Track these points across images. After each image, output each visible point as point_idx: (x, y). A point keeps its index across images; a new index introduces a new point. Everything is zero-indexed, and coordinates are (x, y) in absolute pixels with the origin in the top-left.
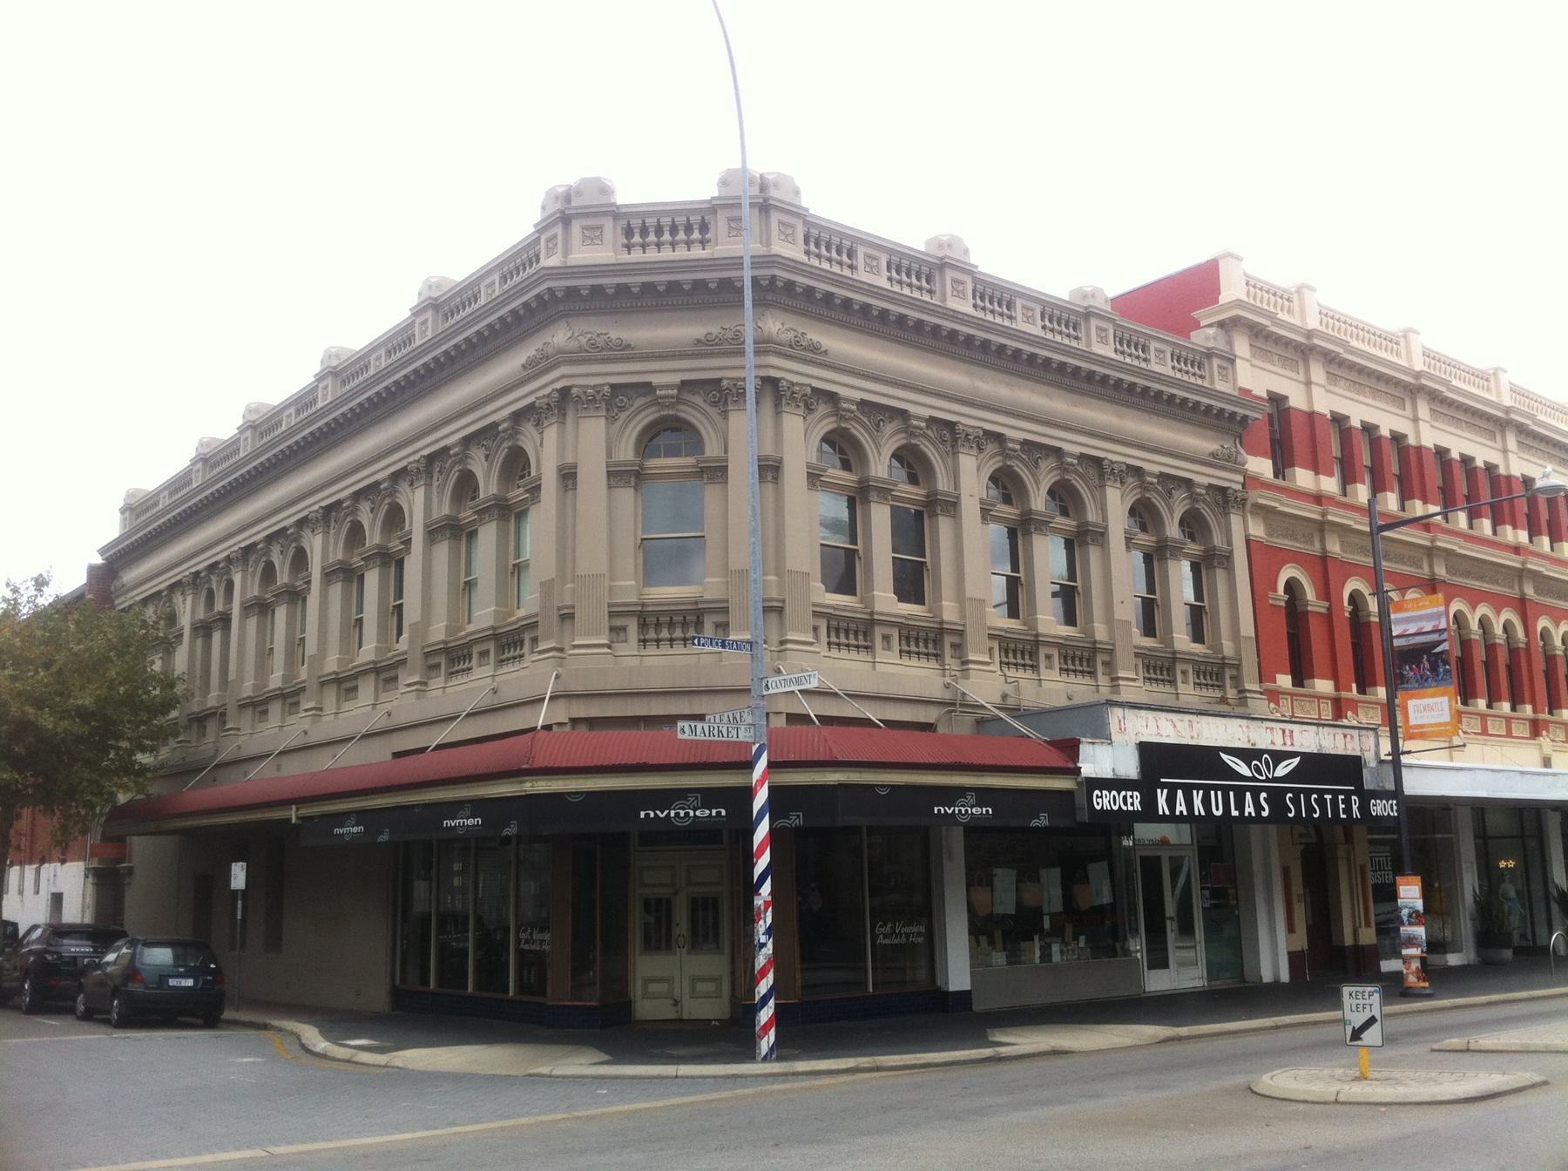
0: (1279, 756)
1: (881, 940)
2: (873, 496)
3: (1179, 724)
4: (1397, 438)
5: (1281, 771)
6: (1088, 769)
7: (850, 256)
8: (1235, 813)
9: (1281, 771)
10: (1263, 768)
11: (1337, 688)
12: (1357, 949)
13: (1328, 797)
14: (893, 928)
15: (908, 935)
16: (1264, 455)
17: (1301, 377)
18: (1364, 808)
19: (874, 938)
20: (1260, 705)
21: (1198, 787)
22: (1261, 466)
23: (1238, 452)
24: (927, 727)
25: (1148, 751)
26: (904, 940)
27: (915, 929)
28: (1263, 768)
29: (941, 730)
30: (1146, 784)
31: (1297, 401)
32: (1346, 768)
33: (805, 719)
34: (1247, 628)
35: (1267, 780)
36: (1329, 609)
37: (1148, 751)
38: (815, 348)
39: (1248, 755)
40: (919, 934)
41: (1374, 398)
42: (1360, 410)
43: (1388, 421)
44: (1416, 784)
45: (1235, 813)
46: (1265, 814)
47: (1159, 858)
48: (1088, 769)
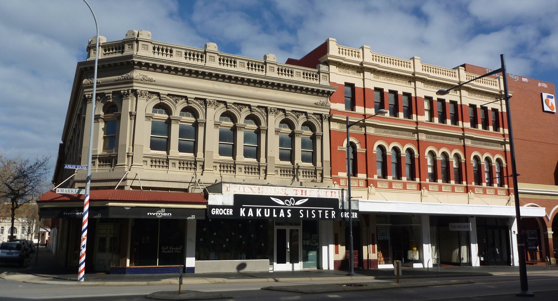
0: (297, 199)
1: (163, 251)
2: (173, 121)
3: (253, 189)
4: (408, 95)
5: (299, 203)
6: (210, 202)
7: (291, 73)
8: (275, 216)
9: (299, 203)
10: (290, 202)
11: (367, 177)
12: (368, 260)
13: (320, 211)
14: (169, 248)
15: (174, 250)
16: (342, 103)
17: (362, 77)
18: (337, 215)
19: (160, 250)
20: (328, 181)
21: (266, 208)
22: (341, 107)
23: (327, 102)
24: (186, 190)
25: (237, 198)
26: (172, 252)
27: (177, 249)
28: (290, 202)
29: (190, 191)
30: (236, 207)
31: (359, 84)
32: (333, 203)
33: (138, 188)
34: (327, 157)
35: (292, 206)
36: (366, 151)
37: (237, 198)
38: (151, 80)
39: (283, 198)
40: (179, 250)
41: (397, 81)
42: (387, 85)
43: (402, 87)
44: (364, 207)
45: (275, 216)
46: (289, 216)
47: (285, 230)
48: (210, 202)
